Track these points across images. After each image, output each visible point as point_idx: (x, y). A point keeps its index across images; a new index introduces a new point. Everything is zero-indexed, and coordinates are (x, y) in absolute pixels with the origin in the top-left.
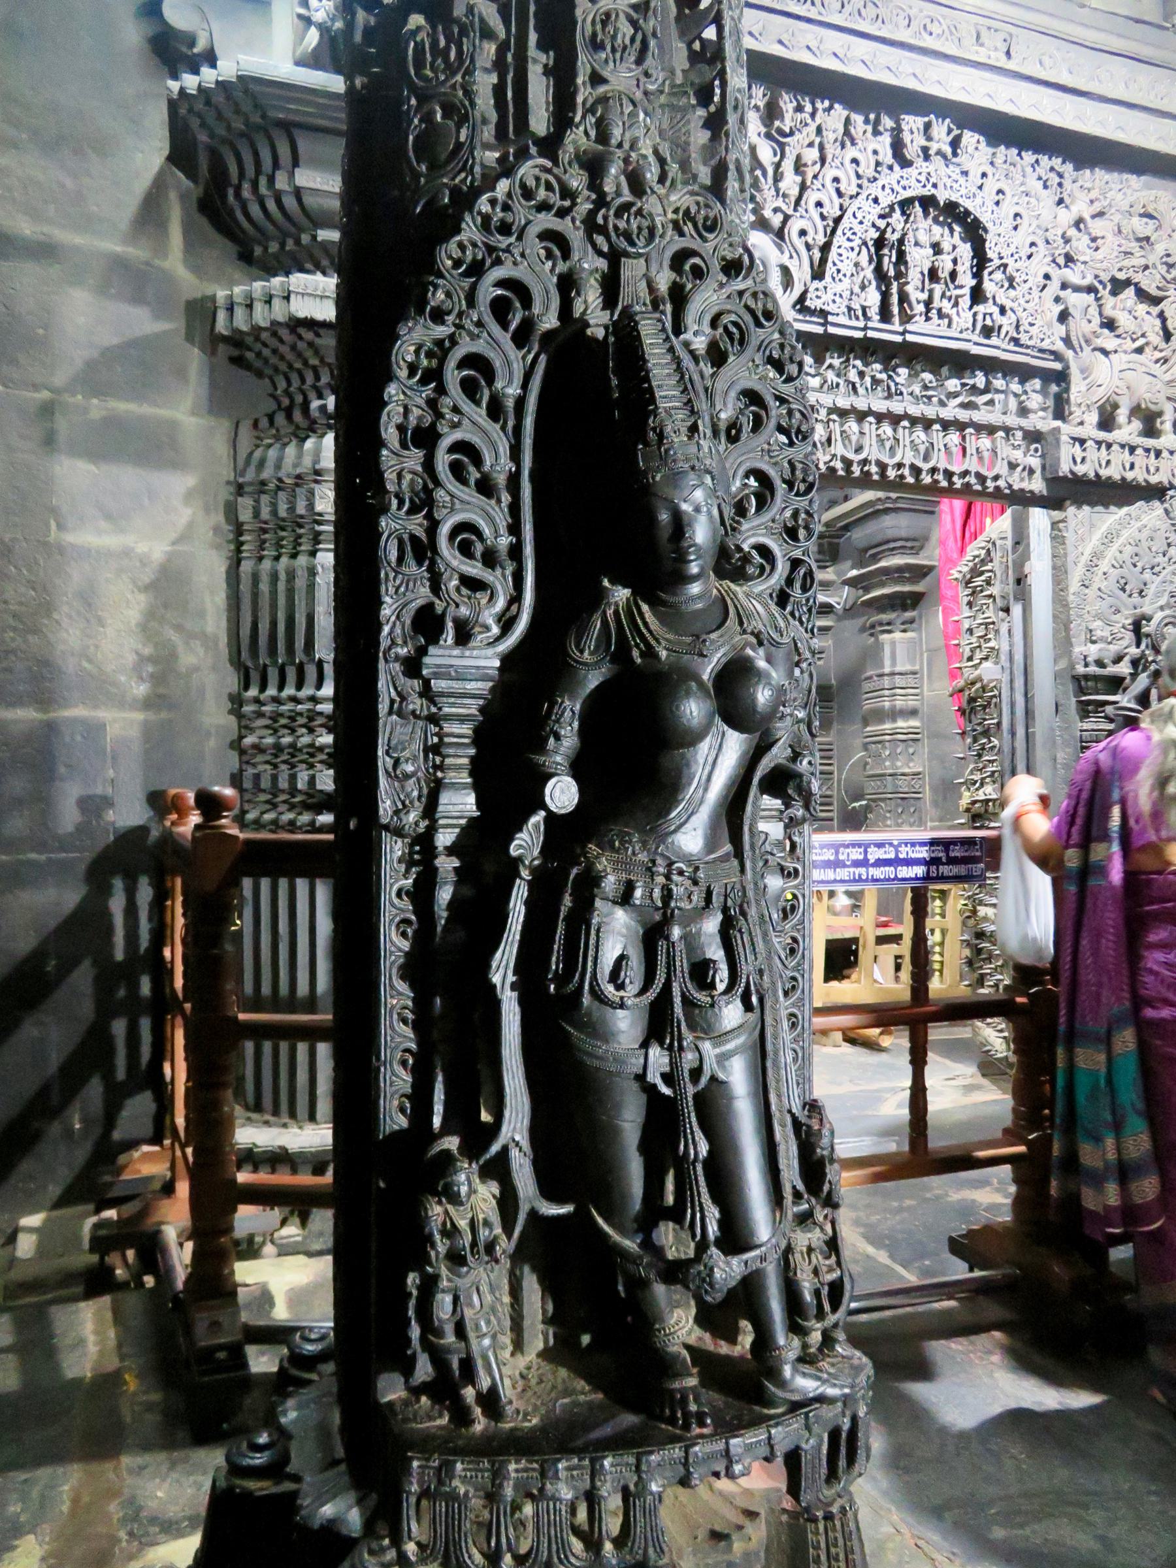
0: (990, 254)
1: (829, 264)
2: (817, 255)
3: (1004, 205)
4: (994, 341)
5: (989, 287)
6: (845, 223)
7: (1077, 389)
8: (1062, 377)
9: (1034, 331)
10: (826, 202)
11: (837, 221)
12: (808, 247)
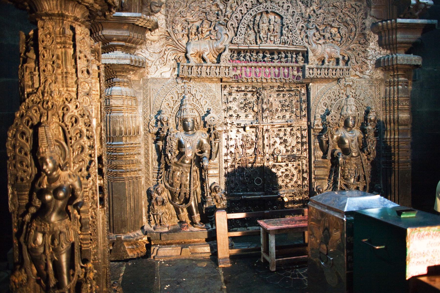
0: (284, 24)
1: (238, 32)
2: (236, 29)
3: (289, 10)
4: (286, 45)
5: (284, 32)
6: (242, 21)
7: (310, 54)
8: (307, 52)
9: (297, 42)
10: (238, 16)
11: (241, 20)
12: (234, 28)
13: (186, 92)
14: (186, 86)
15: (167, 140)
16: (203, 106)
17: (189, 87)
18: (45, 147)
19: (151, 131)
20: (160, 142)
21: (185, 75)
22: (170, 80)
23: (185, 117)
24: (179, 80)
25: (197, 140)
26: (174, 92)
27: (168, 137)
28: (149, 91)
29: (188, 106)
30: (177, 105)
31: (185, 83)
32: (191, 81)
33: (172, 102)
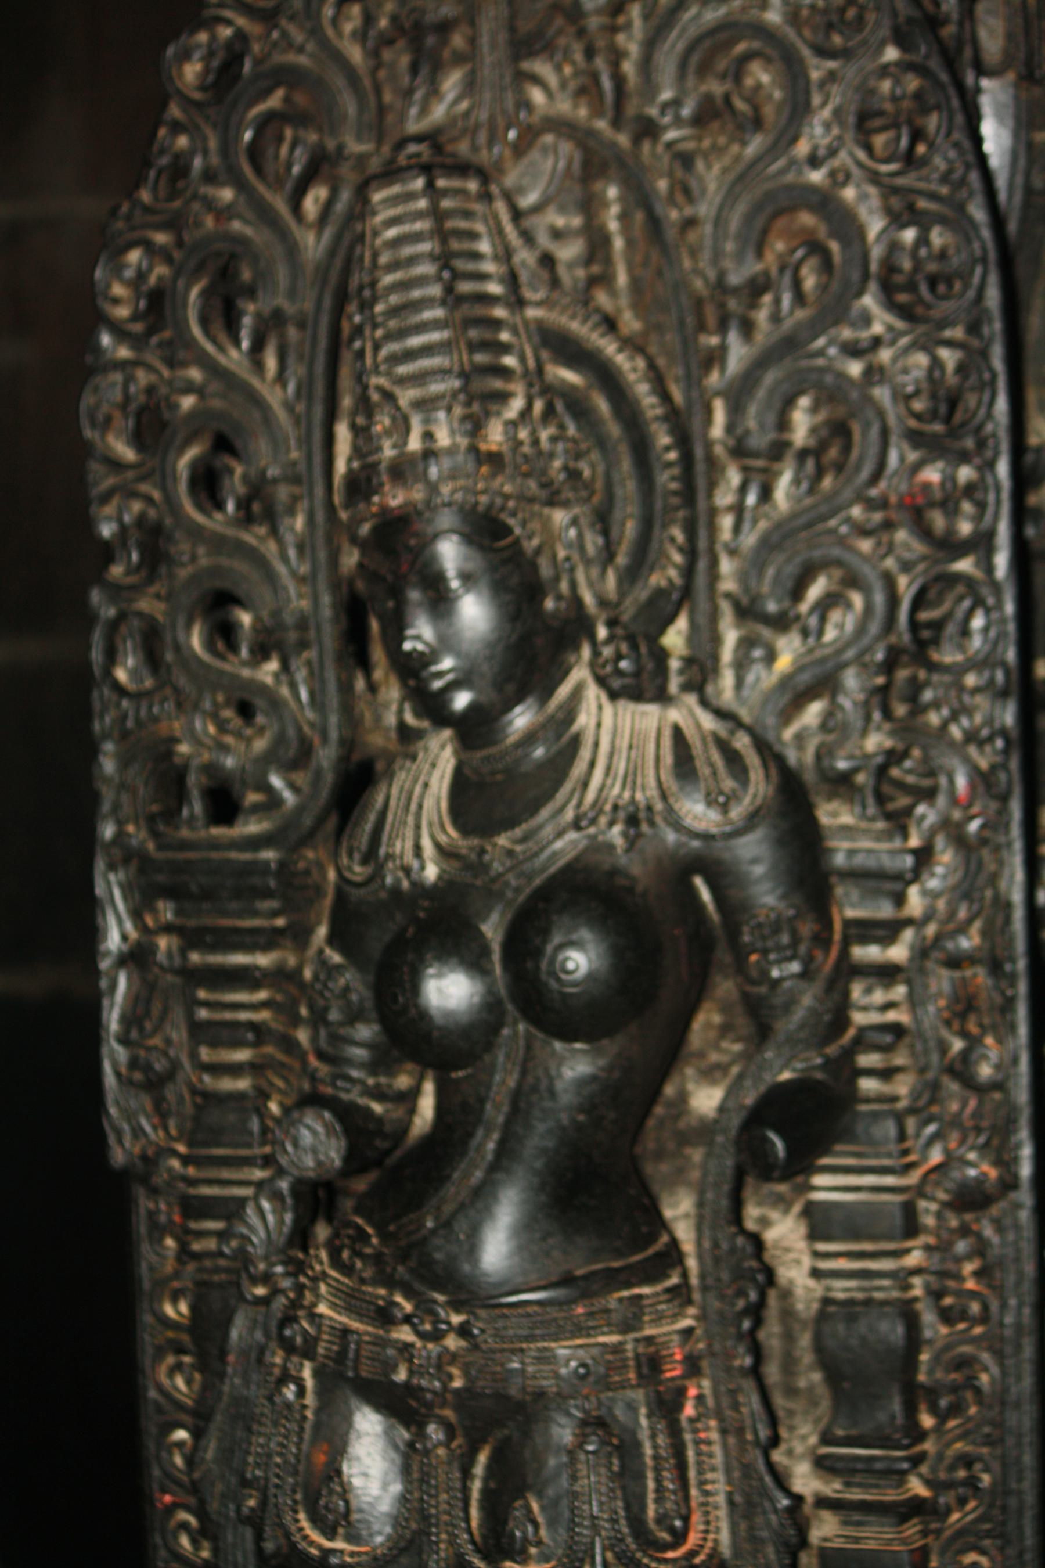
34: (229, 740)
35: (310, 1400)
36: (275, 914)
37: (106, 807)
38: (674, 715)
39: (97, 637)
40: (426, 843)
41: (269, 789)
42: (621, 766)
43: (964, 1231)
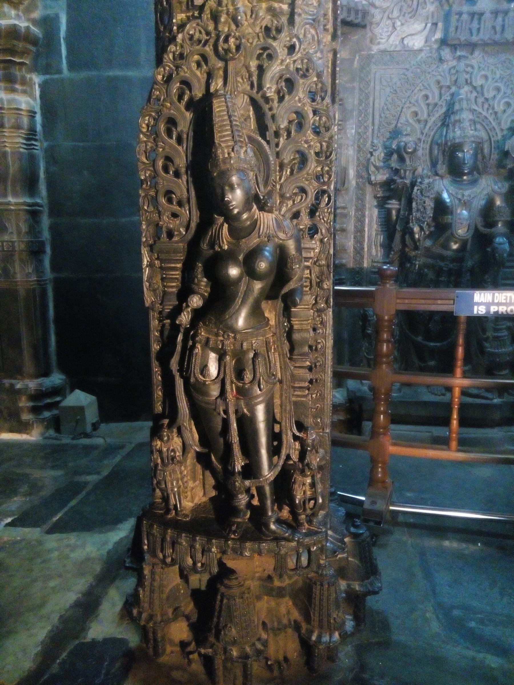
13: (462, 81)
14: (462, 65)
15: (414, 195)
16: (499, 115)
17: (469, 69)
18: (227, 147)
19: (373, 178)
20: (394, 201)
21: (463, 38)
22: (423, 54)
23: (457, 141)
24: (446, 53)
25: (482, 196)
26: (432, 82)
27: (416, 188)
28: (372, 84)
29: (466, 116)
30: (437, 115)
31: (459, 58)
32: (477, 53)
33: (425, 108)
34: (171, 221)
35: (200, 352)
36: (181, 257)
37: (144, 235)
38: (274, 216)
39: (141, 200)
40: (225, 241)
41: (180, 232)
42: (266, 226)
43: (319, 316)
